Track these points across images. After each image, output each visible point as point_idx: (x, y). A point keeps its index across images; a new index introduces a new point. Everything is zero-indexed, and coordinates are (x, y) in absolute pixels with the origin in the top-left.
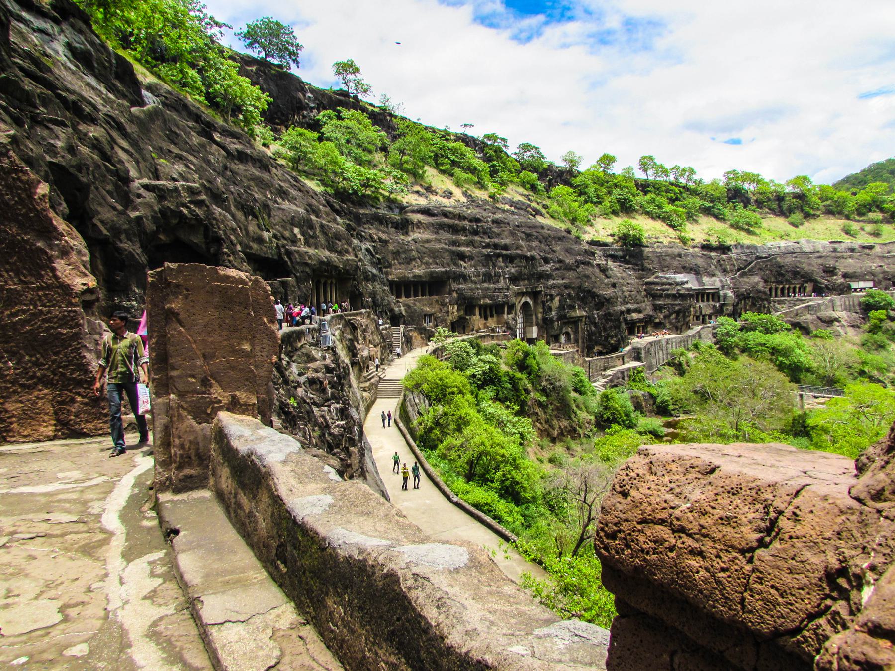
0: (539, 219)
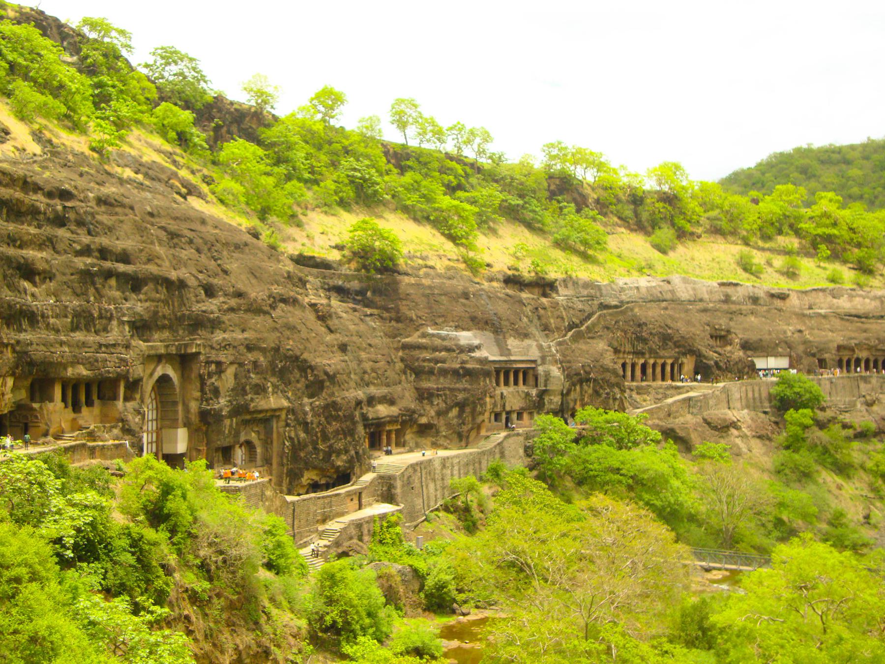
0: (195, 202)
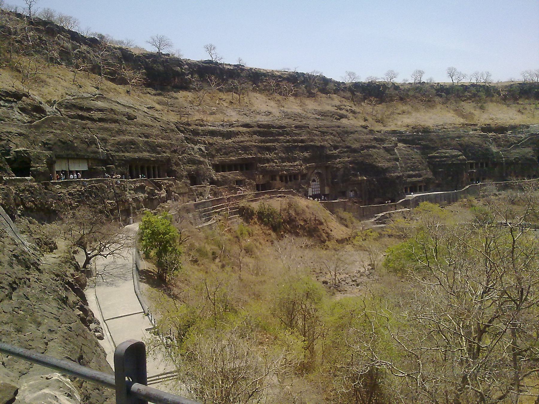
0: (344, 121)
